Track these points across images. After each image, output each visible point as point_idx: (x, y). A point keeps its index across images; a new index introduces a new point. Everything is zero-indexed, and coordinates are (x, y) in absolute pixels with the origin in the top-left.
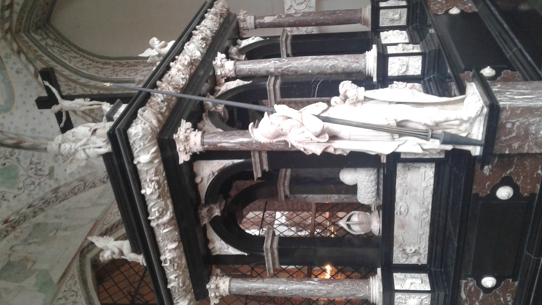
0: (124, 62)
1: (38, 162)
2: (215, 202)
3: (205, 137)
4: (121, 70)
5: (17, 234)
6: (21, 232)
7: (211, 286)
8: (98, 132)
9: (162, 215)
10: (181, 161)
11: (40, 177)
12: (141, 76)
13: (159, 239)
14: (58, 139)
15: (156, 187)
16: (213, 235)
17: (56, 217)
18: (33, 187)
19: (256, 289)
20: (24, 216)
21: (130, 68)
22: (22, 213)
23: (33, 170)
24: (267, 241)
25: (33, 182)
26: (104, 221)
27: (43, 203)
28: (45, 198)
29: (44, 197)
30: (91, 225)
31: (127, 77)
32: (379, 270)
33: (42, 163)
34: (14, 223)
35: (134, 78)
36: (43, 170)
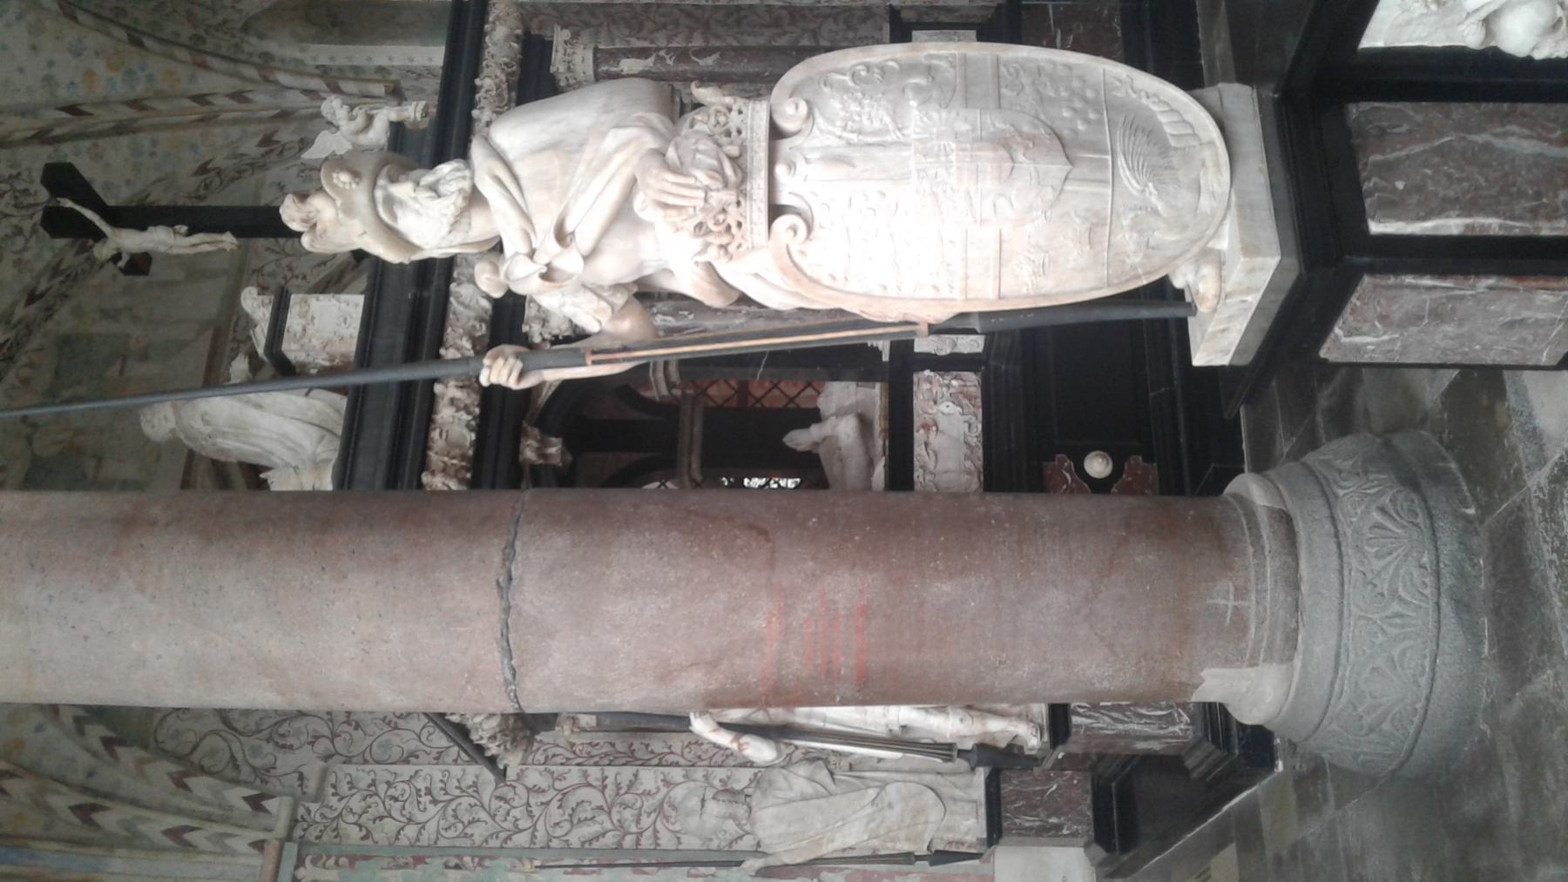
1: (14, 172)
5: (25, 372)
6: (31, 365)
11: (31, 211)
14: (166, 418)
17: (105, 314)
18: (20, 241)
20: (27, 326)
22: (20, 322)
23: (7, 198)
25: (16, 227)
26: (235, 331)
27: (62, 282)
28: (63, 267)
29: (60, 263)
30: (204, 344)
33: (25, 175)
34: (9, 349)
36: (32, 191)
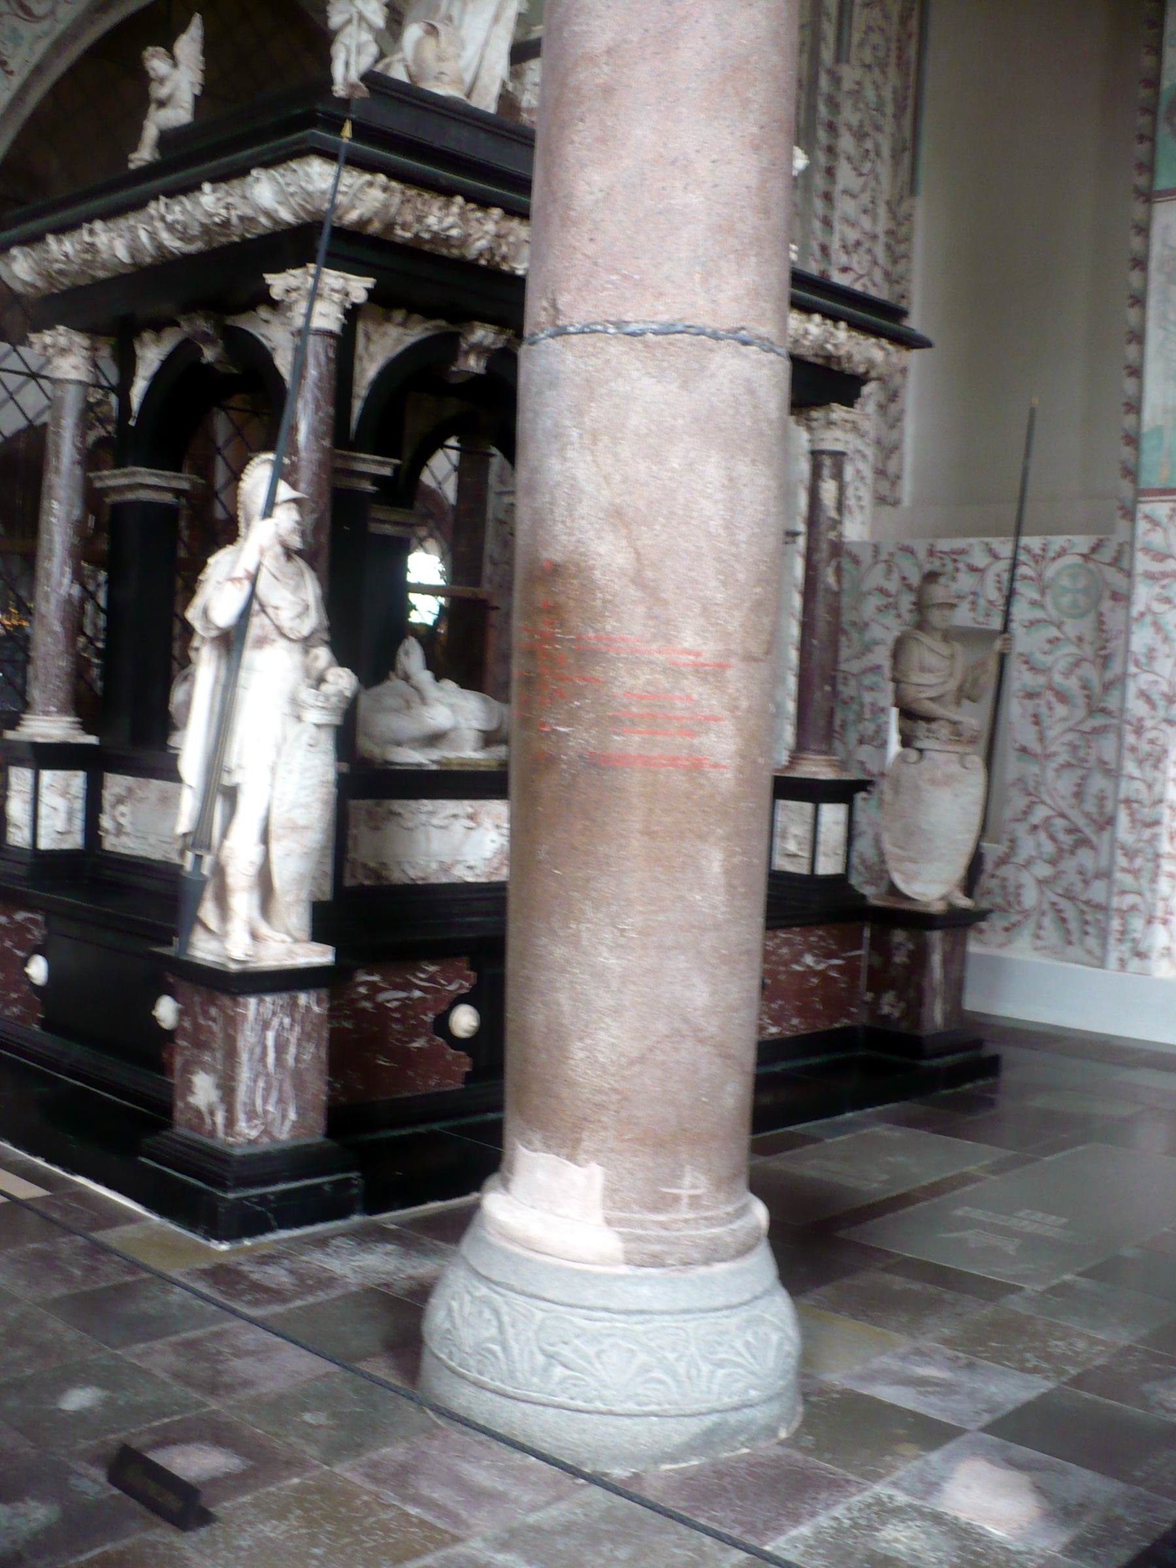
0: (914, 24)
2: (227, 349)
3: (318, 338)
4: (886, 17)
7: (60, 336)
8: (430, 43)
9: (170, 227)
10: (270, 278)
12: (858, 83)
13: (132, 220)
15: (217, 220)
16: (170, 341)
19: (57, 445)
21: (894, 46)
24: (157, 475)
31: (856, 37)
32: (92, 740)
35: (848, 61)
